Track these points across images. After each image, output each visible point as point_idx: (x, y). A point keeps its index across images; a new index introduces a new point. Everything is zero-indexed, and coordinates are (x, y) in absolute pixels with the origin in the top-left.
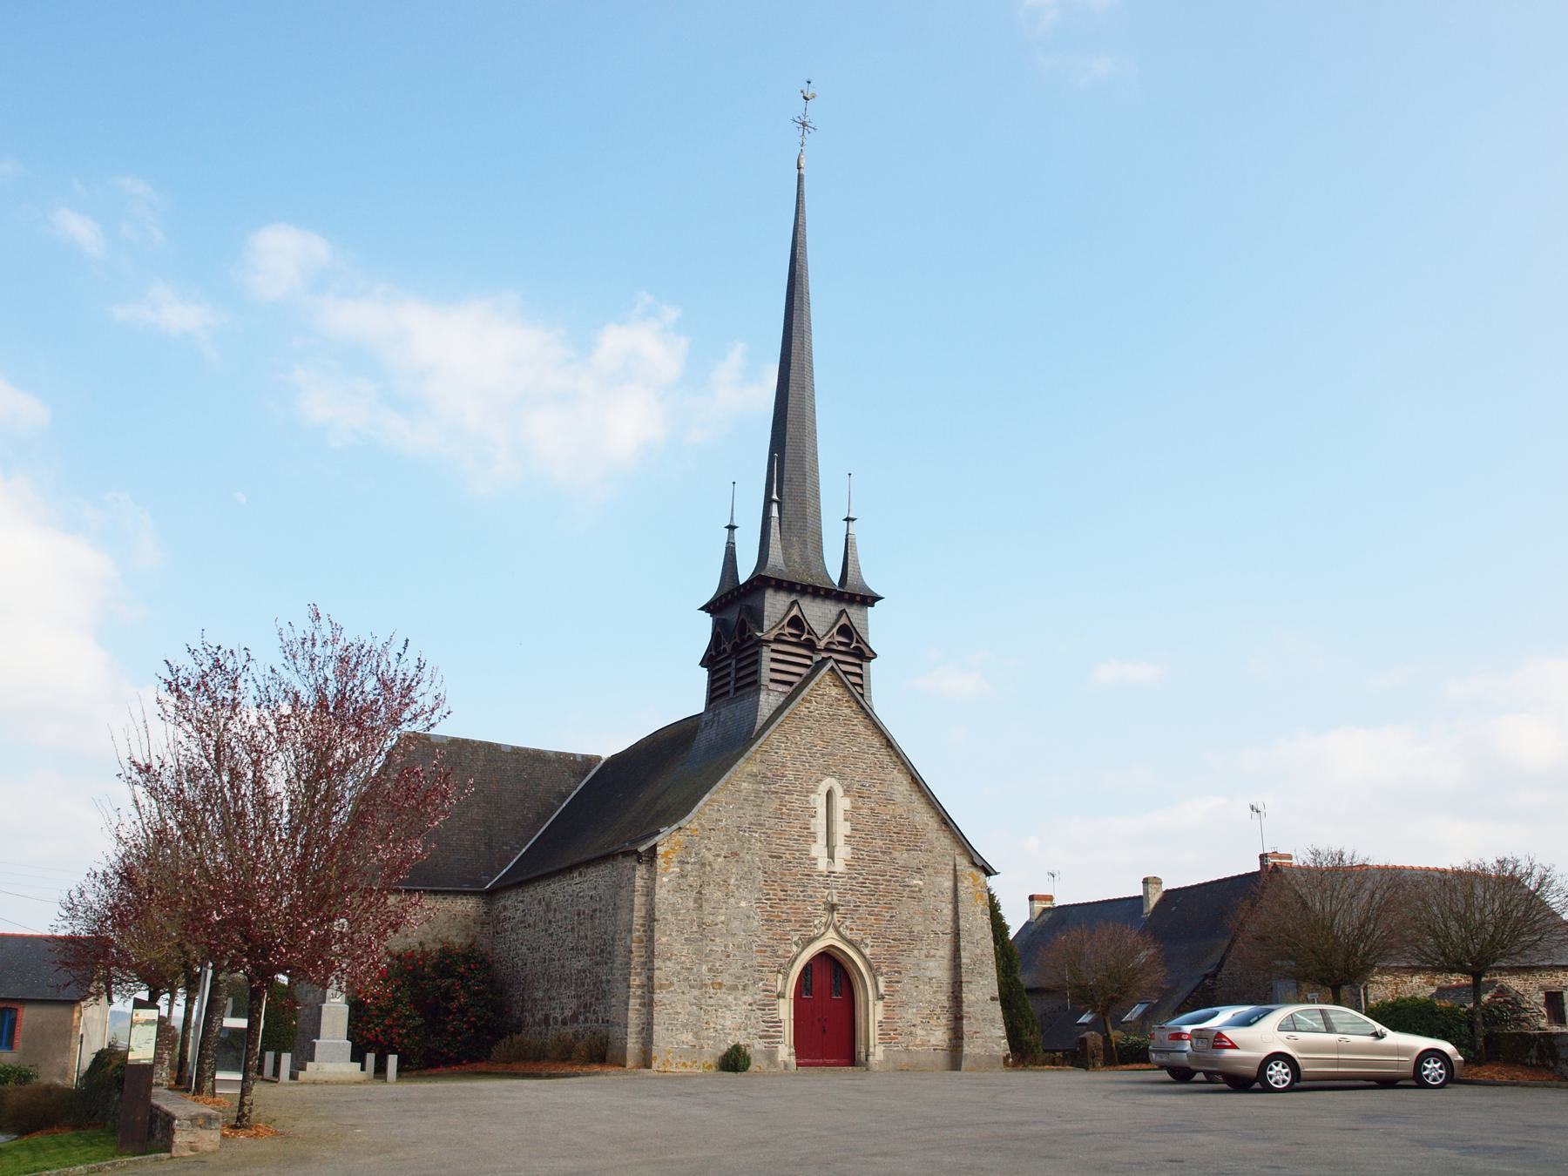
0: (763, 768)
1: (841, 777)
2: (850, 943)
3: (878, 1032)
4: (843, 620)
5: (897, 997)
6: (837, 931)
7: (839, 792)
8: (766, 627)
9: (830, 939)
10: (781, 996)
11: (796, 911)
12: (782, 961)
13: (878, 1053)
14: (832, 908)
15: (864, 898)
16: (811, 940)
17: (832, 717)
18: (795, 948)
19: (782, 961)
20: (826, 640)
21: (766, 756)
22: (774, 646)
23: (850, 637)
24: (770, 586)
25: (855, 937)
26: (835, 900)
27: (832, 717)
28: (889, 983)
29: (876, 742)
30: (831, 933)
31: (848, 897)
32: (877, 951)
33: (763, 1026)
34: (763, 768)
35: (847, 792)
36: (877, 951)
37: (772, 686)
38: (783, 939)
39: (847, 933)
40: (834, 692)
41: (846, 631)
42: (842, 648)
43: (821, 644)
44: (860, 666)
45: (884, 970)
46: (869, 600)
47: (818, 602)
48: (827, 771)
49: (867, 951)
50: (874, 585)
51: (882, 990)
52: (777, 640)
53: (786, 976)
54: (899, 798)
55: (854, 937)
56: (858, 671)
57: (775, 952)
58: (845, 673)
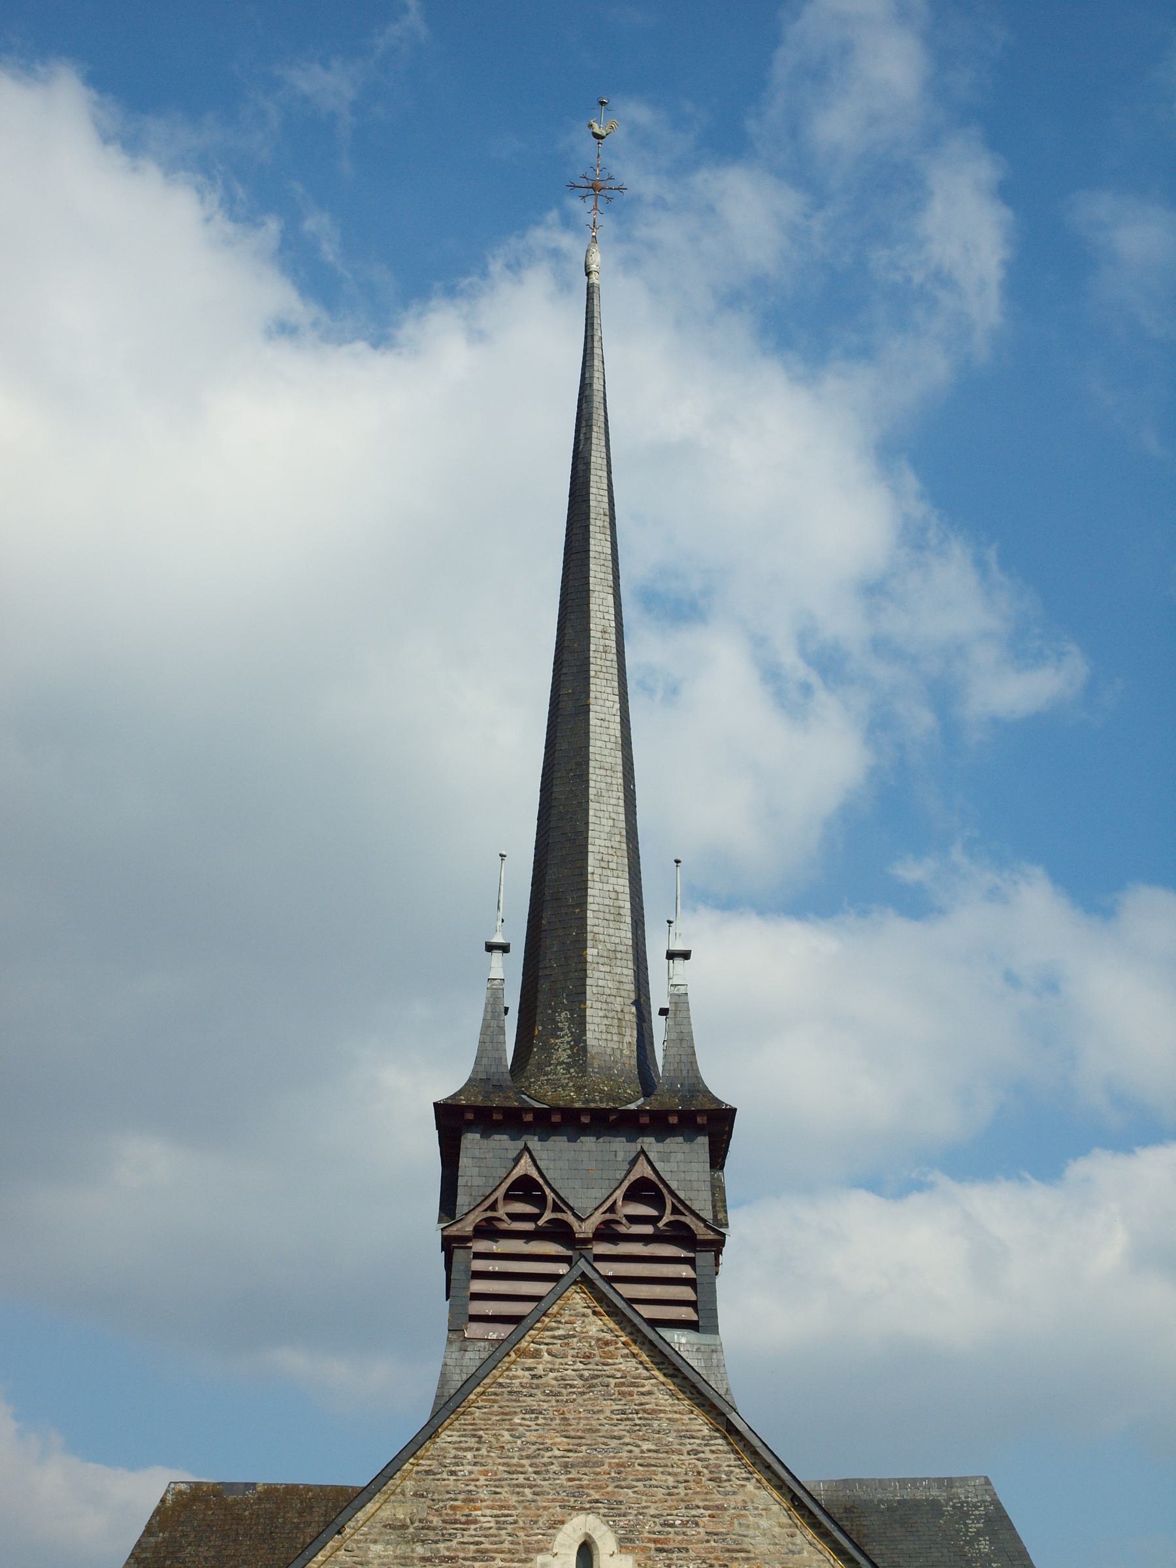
0: (420, 1509)
1: (612, 1511)
4: (642, 1170)
7: (606, 1543)
8: (461, 1210)
17: (590, 1383)
20: (597, 1218)
21: (429, 1483)
22: (481, 1246)
23: (657, 1201)
24: (470, 1126)
27: (590, 1383)
29: (701, 1425)
34: (420, 1509)
35: (625, 1543)
37: (474, 1330)
40: (597, 1326)
41: (645, 1190)
42: (648, 1229)
43: (584, 1230)
44: (690, 1262)
46: (713, 1124)
47: (588, 1143)
48: (577, 1501)
50: (721, 1081)
52: (488, 1230)
54: (760, 1545)
56: (685, 1271)
58: (610, 1280)
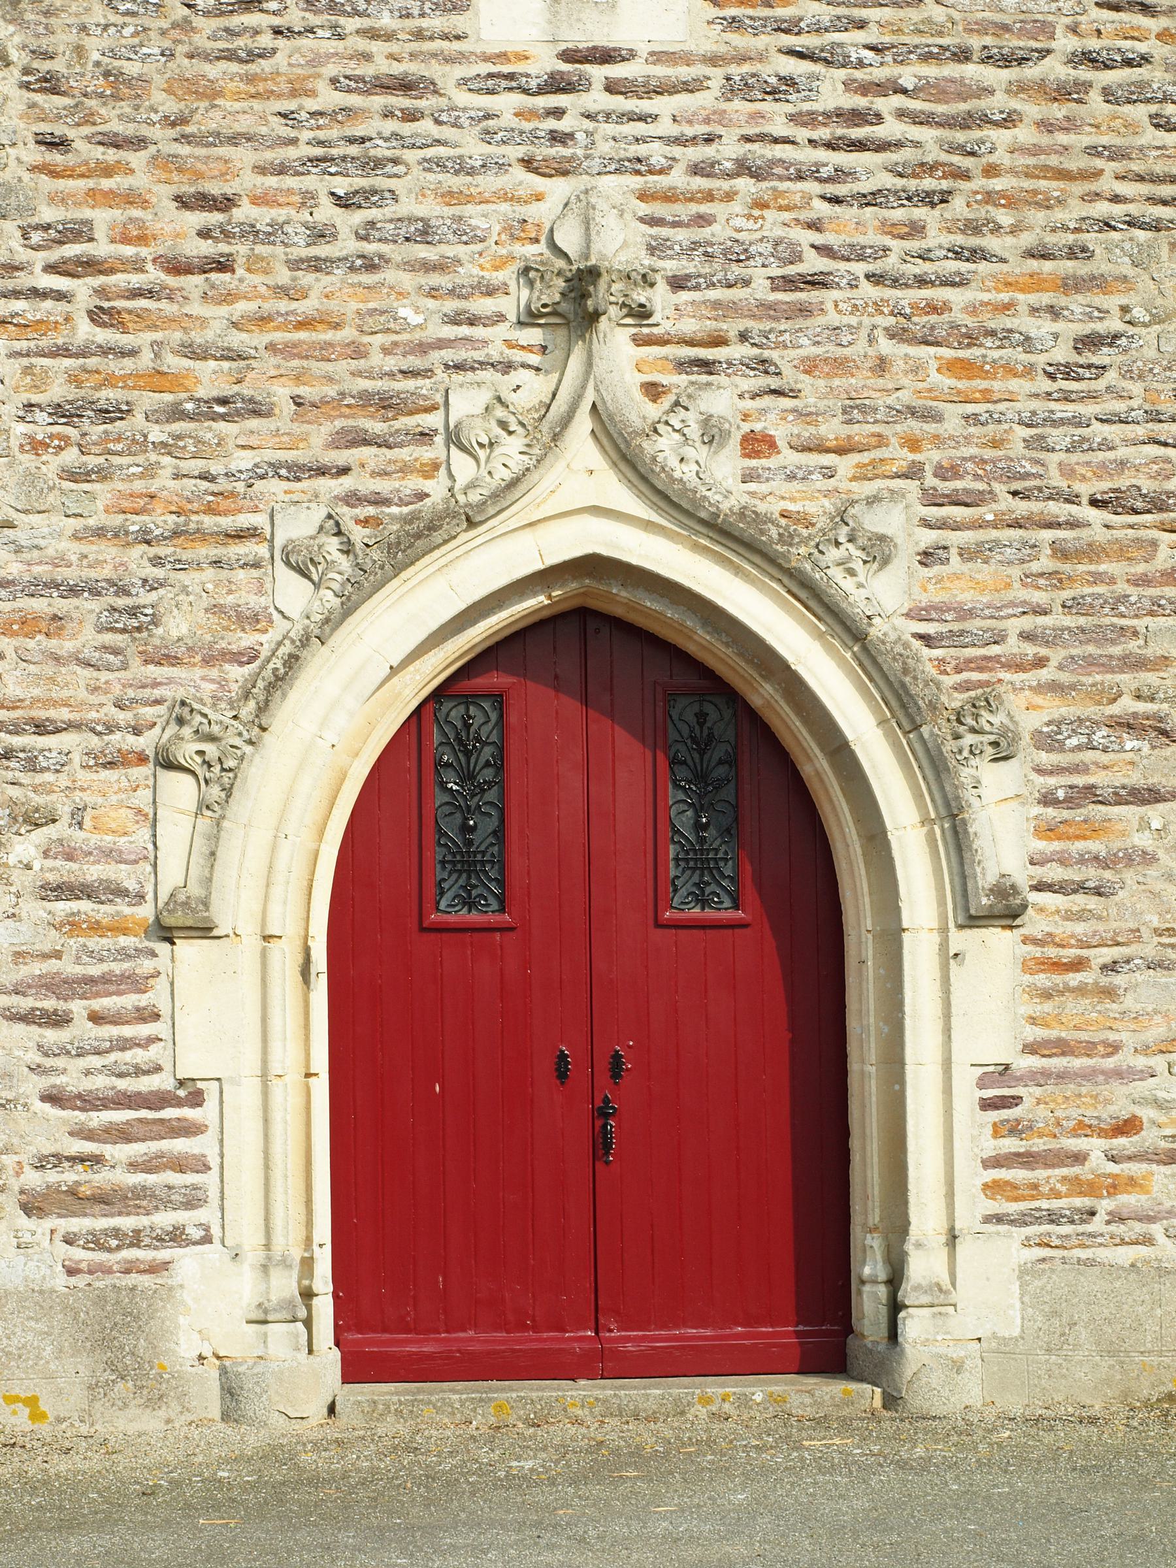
2: (735, 537)
3: (976, 1135)
5: (1136, 904)
6: (626, 455)
9: (586, 511)
10: (181, 925)
11: (307, 338)
12: (191, 681)
13: (967, 1285)
14: (575, 303)
15: (854, 226)
16: (418, 537)
18: (293, 596)
19: (191, 681)
25: (779, 495)
26: (619, 242)
28: (1071, 802)
30: (582, 471)
31: (729, 222)
32: (962, 582)
33: (52, 1130)
36: (962, 582)
38: (211, 527)
39: (722, 479)
45: (1026, 710)
49: (884, 597)
51: (1007, 841)
53: (221, 781)
55: (775, 498)
57: (135, 622)
